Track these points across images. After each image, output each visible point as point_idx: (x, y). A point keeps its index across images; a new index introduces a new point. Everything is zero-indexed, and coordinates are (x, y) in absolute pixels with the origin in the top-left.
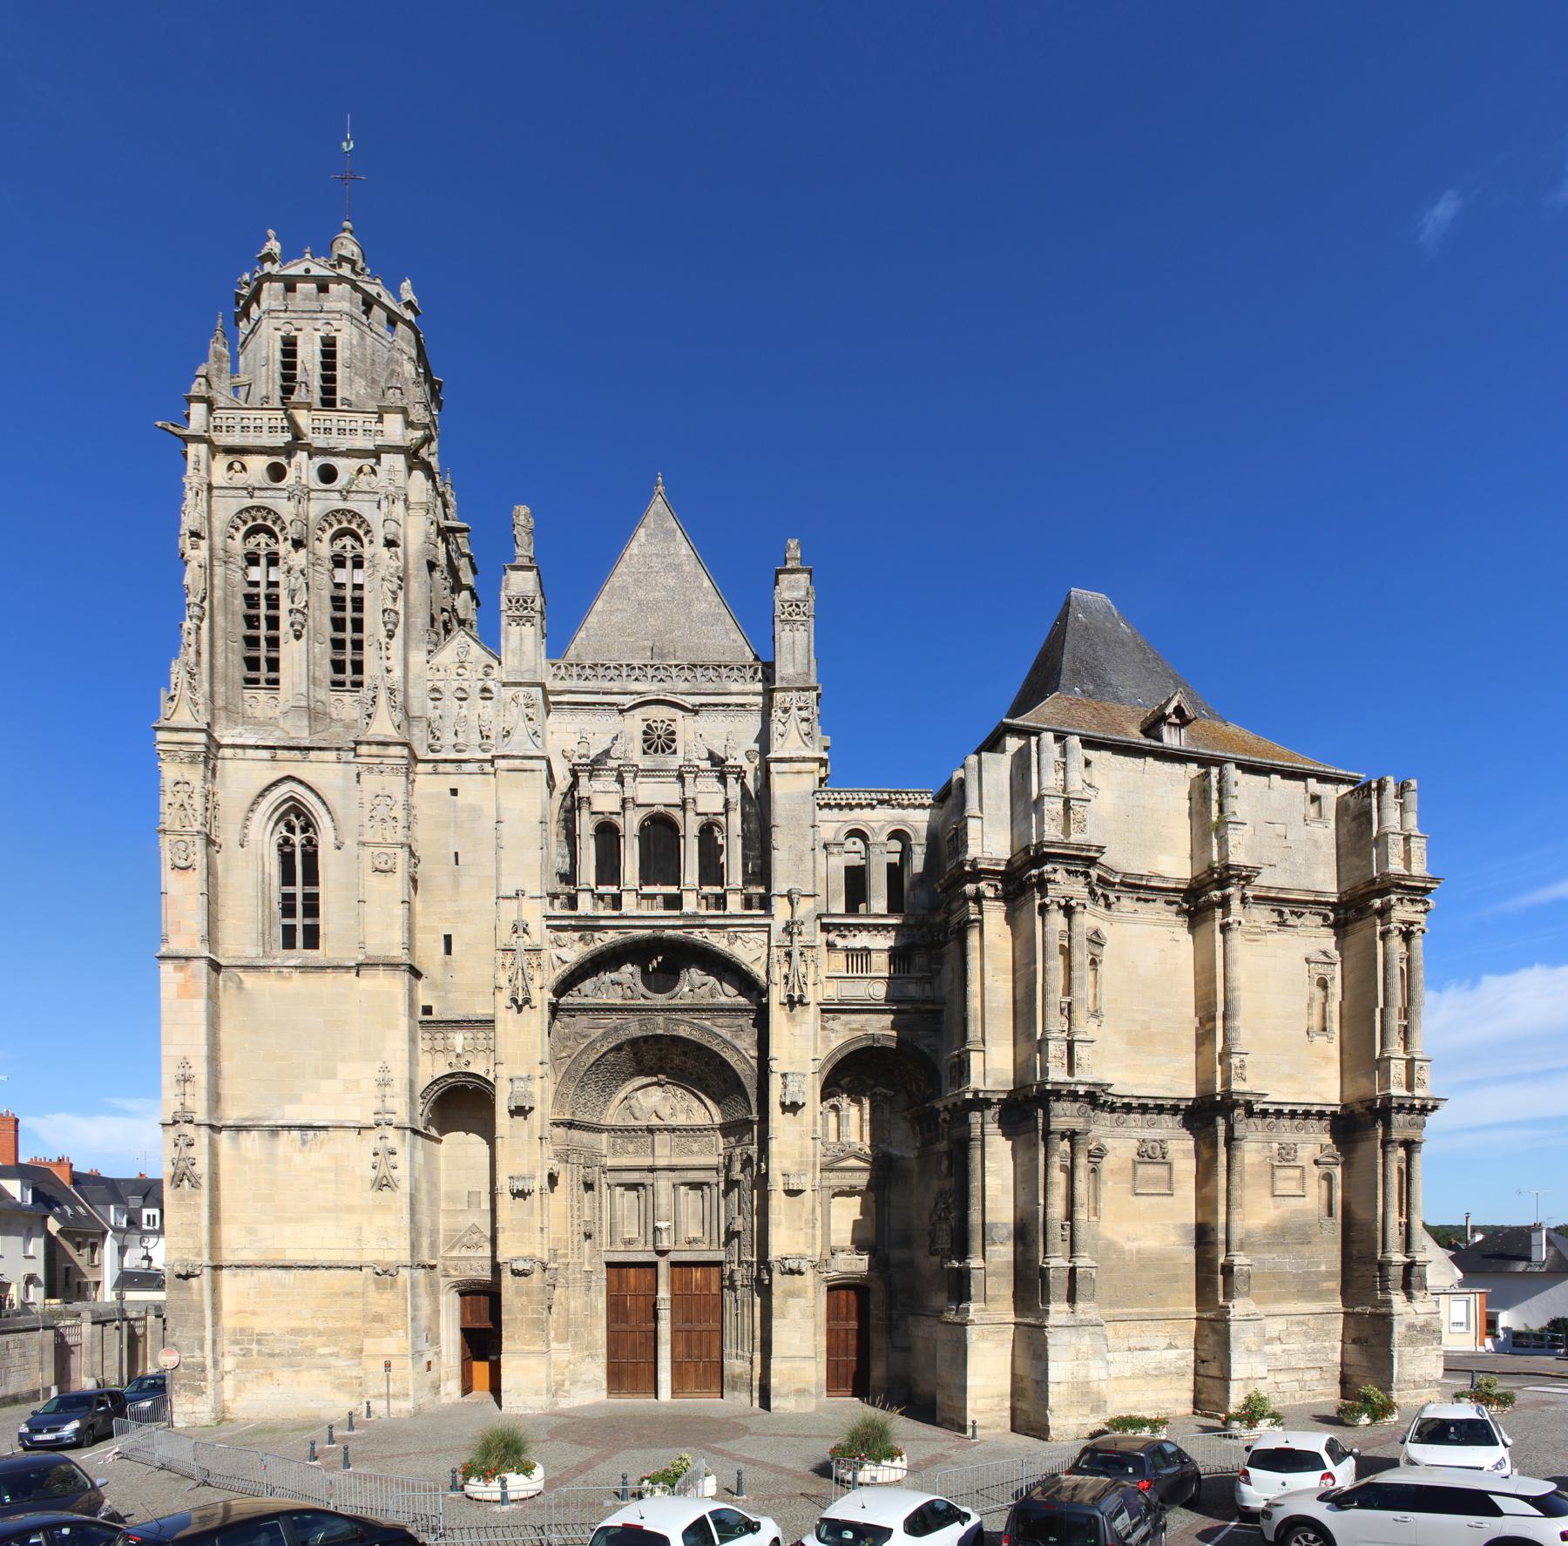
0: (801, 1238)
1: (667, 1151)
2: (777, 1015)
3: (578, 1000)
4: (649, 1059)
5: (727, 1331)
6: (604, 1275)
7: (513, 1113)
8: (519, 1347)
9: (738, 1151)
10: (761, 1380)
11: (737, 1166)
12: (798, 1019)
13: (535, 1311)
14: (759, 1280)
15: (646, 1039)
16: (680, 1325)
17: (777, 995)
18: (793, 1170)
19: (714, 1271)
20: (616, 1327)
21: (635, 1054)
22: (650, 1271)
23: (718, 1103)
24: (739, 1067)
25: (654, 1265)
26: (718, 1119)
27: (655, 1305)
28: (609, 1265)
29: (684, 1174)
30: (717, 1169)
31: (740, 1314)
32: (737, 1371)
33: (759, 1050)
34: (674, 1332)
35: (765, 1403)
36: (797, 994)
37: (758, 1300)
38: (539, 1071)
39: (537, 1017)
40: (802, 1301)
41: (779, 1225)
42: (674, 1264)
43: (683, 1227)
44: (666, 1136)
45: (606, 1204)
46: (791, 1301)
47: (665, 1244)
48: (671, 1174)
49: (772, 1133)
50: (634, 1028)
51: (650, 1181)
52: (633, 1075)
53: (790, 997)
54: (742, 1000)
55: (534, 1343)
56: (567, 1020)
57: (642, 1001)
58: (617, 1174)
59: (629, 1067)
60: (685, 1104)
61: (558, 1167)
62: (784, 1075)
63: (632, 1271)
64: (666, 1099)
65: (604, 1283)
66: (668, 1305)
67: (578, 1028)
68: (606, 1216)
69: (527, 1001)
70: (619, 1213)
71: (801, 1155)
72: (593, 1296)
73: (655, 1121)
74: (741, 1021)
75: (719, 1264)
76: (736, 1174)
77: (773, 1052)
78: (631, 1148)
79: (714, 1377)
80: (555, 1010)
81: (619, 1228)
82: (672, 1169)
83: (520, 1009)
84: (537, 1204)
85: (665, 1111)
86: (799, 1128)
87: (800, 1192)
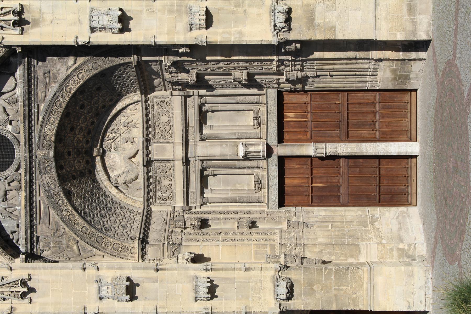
0: (253, 11)
1: (169, 147)
2: (33, 37)
3: (22, 233)
4: (79, 165)
5: (348, 86)
6: (292, 209)
7: (133, 297)
8: (363, 293)
9: (167, 76)
10: (398, 50)
11: (183, 76)
12: (37, 16)
13: (328, 277)
14: (297, 53)
15: (59, 167)
16: (342, 134)
17: (13, 37)
18: (186, 21)
19: (287, 99)
20: (344, 198)
21: (74, 178)
22: (287, 164)
23: (120, 97)
24: (85, 76)
25: (282, 159)
26: (137, 96)
27: (321, 158)
28: (281, 204)
29: (191, 130)
30: (186, 97)
31: (330, 72)
32: (389, 75)
33: (68, 55)
34: (349, 139)
35: (422, 45)
36: (11, 17)
37: (317, 55)
38: (91, 272)
39: (39, 273)
40: (318, 9)
41: (241, 33)
42: (281, 140)
43: (243, 131)
44: (154, 148)
45: (221, 207)
46: (318, 20)
47: (261, 148)
48: (191, 142)
49: (149, 41)
50: (48, 179)
51: (198, 164)
52: (94, 180)
53: (15, 24)
54: (19, 72)
55: (360, 277)
56: (41, 244)
57: (22, 171)
58: (192, 196)
59: (86, 184)
60: (122, 129)
61: (185, 254)
62: (93, 30)
63: (287, 181)
64: (117, 148)
65: (299, 209)
66: (321, 146)
67: (49, 233)
68: (233, 207)
69: (24, 283)
70: (230, 194)
71: (171, 12)
72: (312, 220)
73: (139, 159)
74: (40, 73)
75: (280, 94)
76: (191, 77)
77: (70, 41)
78: (166, 182)
79: (397, 97)
80: (32, 256)
81: (245, 194)
82: (186, 142)
83: (32, 290)
84: (222, 274)
85: (130, 149)
86: (145, 14)
87: (208, 12)
